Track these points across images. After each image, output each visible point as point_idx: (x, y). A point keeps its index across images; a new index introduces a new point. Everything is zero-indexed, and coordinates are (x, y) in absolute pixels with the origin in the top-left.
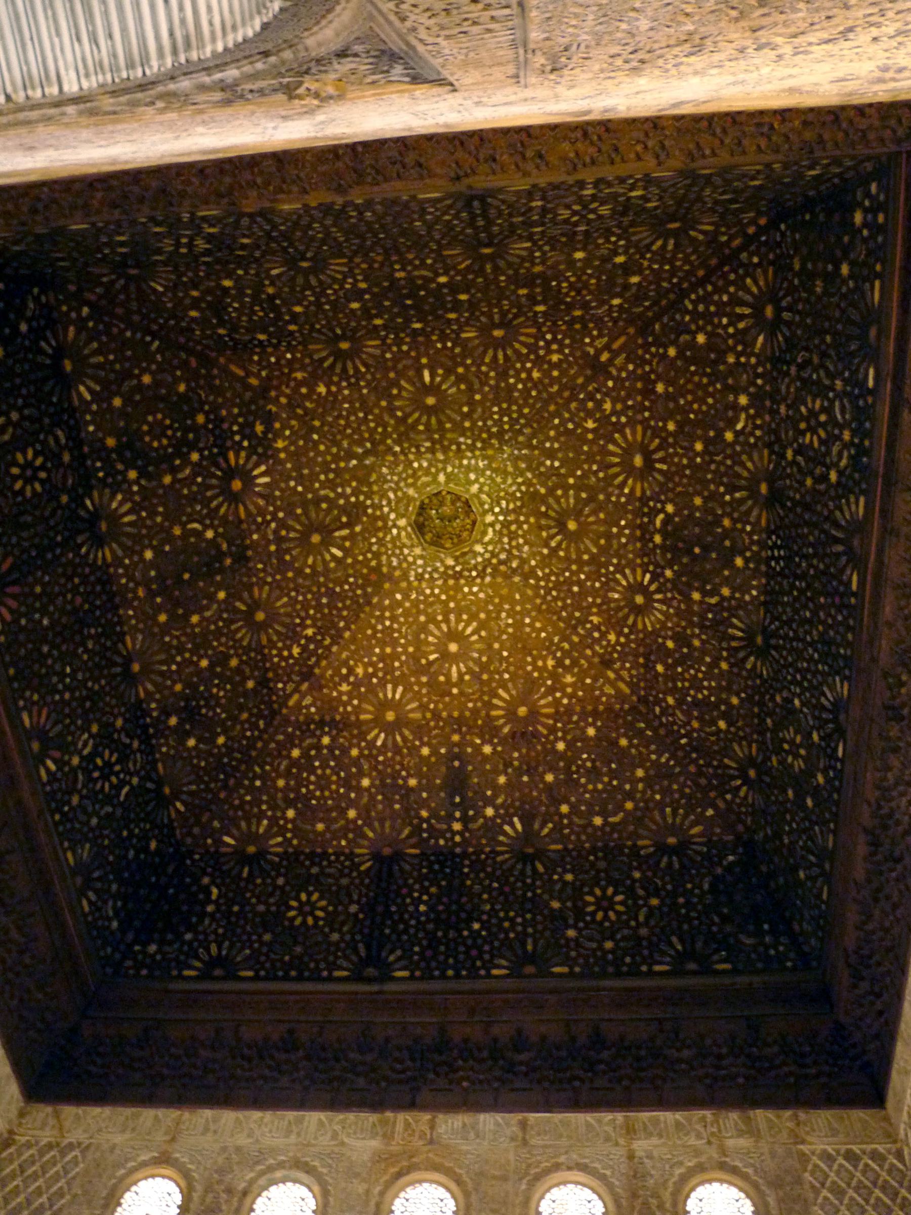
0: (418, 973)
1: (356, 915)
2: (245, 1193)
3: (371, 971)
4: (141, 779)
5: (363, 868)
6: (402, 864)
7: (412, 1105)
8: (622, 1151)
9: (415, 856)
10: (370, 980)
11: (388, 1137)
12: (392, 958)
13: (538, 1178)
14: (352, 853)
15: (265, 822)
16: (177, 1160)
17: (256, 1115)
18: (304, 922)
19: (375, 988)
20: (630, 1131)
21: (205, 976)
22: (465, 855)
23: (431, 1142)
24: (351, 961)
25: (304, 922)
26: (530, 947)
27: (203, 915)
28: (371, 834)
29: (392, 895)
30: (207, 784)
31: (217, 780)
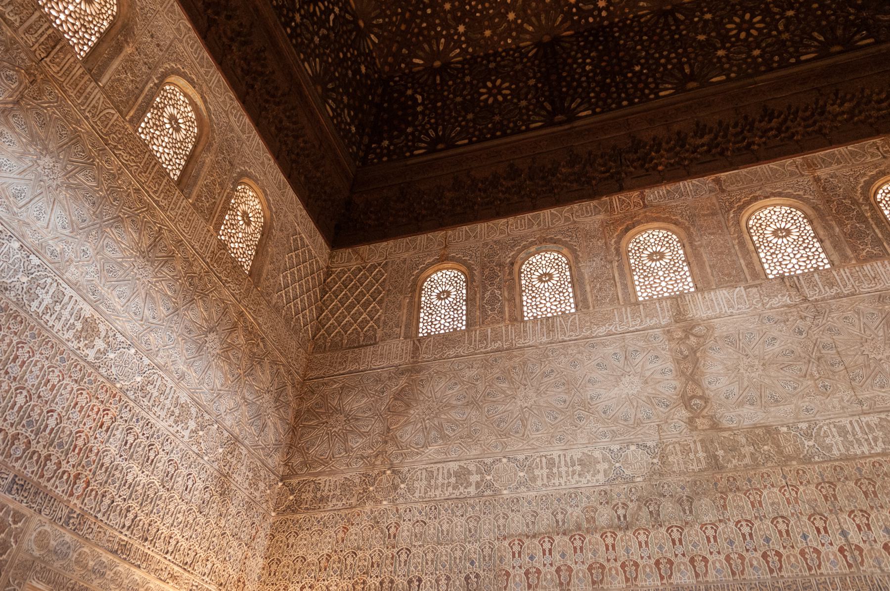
0: (598, 110)
1: (535, 85)
2: (512, 264)
3: (559, 117)
4: (341, 9)
5: (530, 55)
6: (563, 44)
7: (621, 189)
8: (811, 178)
9: (571, 36)
10: (560, 123)
11: (611, 210)
12: (573, 106)
13: (741, 208)
14: (518, 47)
15: (443, 40)
16: (453, 257)
17: (504, 220)
18: (496, 100)
19: (567, 127)
20: (811, 166)
21: (431, 149)
22: (612, 25)
23: (645, 206)
24: (543, 116)
25: (496, 100)
26: (687, 71)
27: (415, 115)
28: (531, 29)
29: (560, 66)
30: (390, 17)
31: (397, 14)
